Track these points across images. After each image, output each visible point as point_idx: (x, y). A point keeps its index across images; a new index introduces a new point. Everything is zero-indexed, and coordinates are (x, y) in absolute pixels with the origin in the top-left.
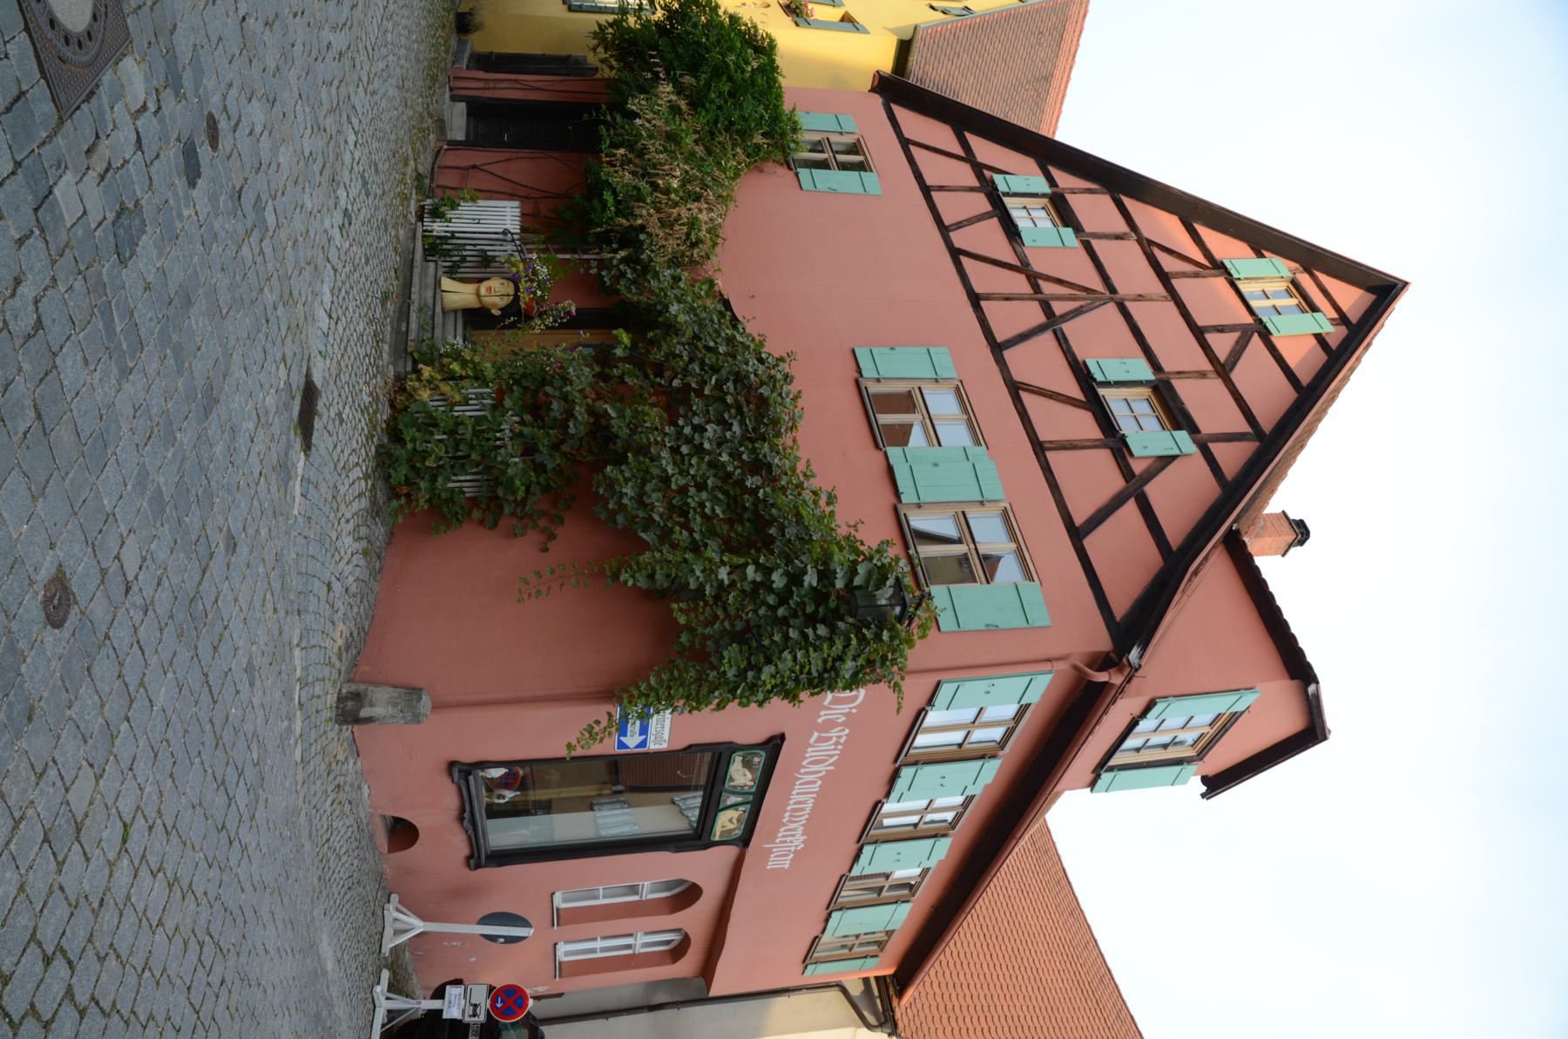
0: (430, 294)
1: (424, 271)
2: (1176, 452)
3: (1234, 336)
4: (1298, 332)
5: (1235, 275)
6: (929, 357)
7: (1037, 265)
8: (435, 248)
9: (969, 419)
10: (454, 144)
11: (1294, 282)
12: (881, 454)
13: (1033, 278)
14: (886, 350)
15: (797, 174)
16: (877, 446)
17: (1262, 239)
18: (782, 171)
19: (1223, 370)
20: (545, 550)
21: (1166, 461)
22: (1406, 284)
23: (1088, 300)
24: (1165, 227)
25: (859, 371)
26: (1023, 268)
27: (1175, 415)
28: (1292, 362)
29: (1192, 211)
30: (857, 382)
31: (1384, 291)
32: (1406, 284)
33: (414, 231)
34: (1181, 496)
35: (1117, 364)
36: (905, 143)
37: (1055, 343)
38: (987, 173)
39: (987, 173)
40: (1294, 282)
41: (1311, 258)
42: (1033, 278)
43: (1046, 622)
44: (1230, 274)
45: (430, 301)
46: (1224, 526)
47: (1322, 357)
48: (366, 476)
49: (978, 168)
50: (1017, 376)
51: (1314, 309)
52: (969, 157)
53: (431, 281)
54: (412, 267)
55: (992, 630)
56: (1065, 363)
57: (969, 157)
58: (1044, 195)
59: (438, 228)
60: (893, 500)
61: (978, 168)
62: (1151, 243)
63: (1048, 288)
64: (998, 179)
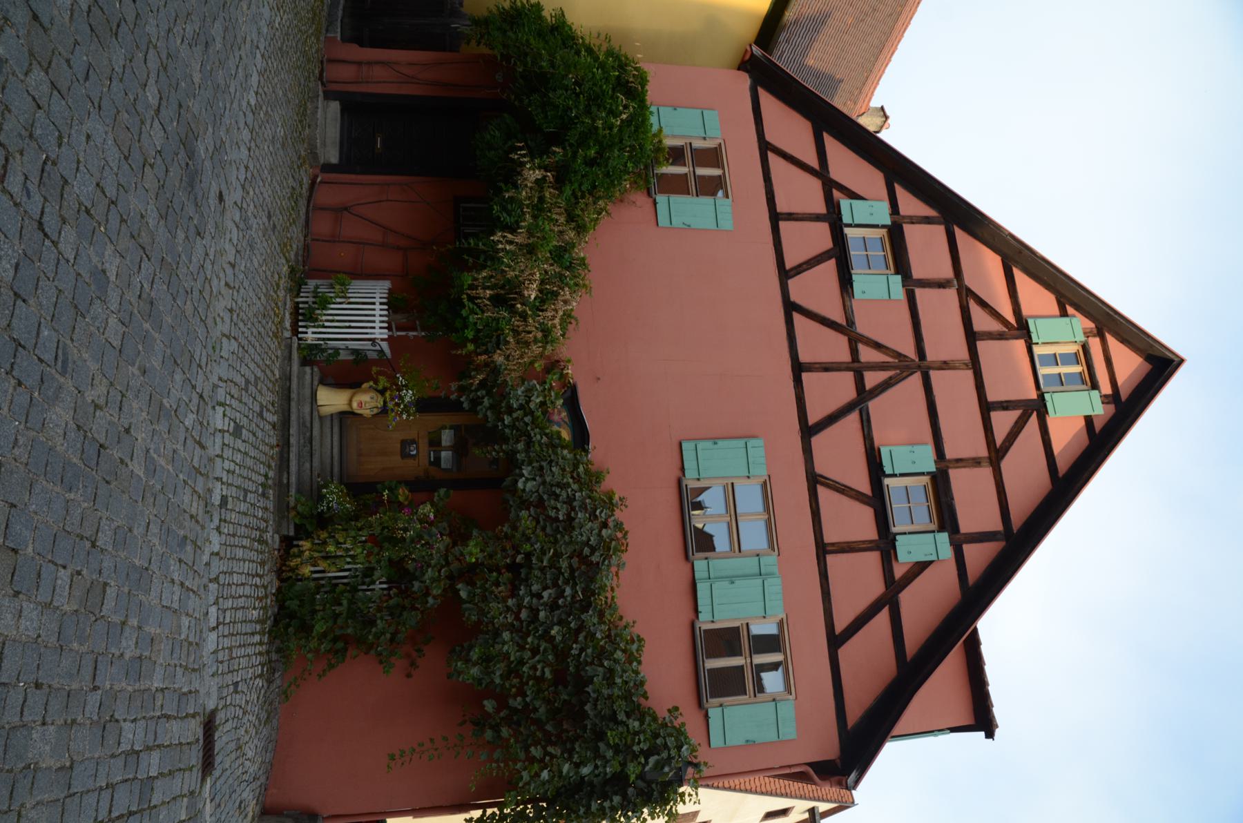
0: (307, 409)
1: (301, 377)
2: (933, 558)
3: (1015, 414)
4: (1072, 410)
5: (1035, 340)
6: (739, 474)
7: (862, 327)
8: (310, 355)
9: (769, 518)
10: (327, 168)
11: (1085, 347)
12: (689, 565)
13: (855, 340)
14: (709, 444)
15: (655, 203)
16: (687, 557)
17: (1070, 295)
18: (640, 198)
19: (996, 454)
20: (409, 676)
21: (921, 567)
22: (1182, 361)
23: (901, 367)
24: (985, 269)
25: (683, 469)
26: (847, 329)
27: (946, 518)
28: (1057, 448)
29: (1017, 257)
30: (679, 482)
31: (1161, 366)
32: (1182, 361)
33: (290, 347)
34: (923, 606)
35: (909, 458)
36: (765, 147)
37: (858, 426)
38: (836, 194)
39: (836, 194)
40: (1085, 347)
41: (1108, 322)
42: (855, 340)
43: (794, 736)
44: (1030, 337)
45: (308, 418)
46: (957, 631)
47: (1084, 441)
48: (261, 621)
49: (829, 186)
50: (820, 468)
51: (1095, 386)
52: (821, 172)
53: (307, 392)
54: (289, 399)
55: (750, 744)
56: (861, 440)
57: (821, 172)
58: (883, 226)
59: (311, 335)
60: (691, 615)
61: (829, 186)
62: (970, 292)
63: (867, 354)
64: (845, 204)
